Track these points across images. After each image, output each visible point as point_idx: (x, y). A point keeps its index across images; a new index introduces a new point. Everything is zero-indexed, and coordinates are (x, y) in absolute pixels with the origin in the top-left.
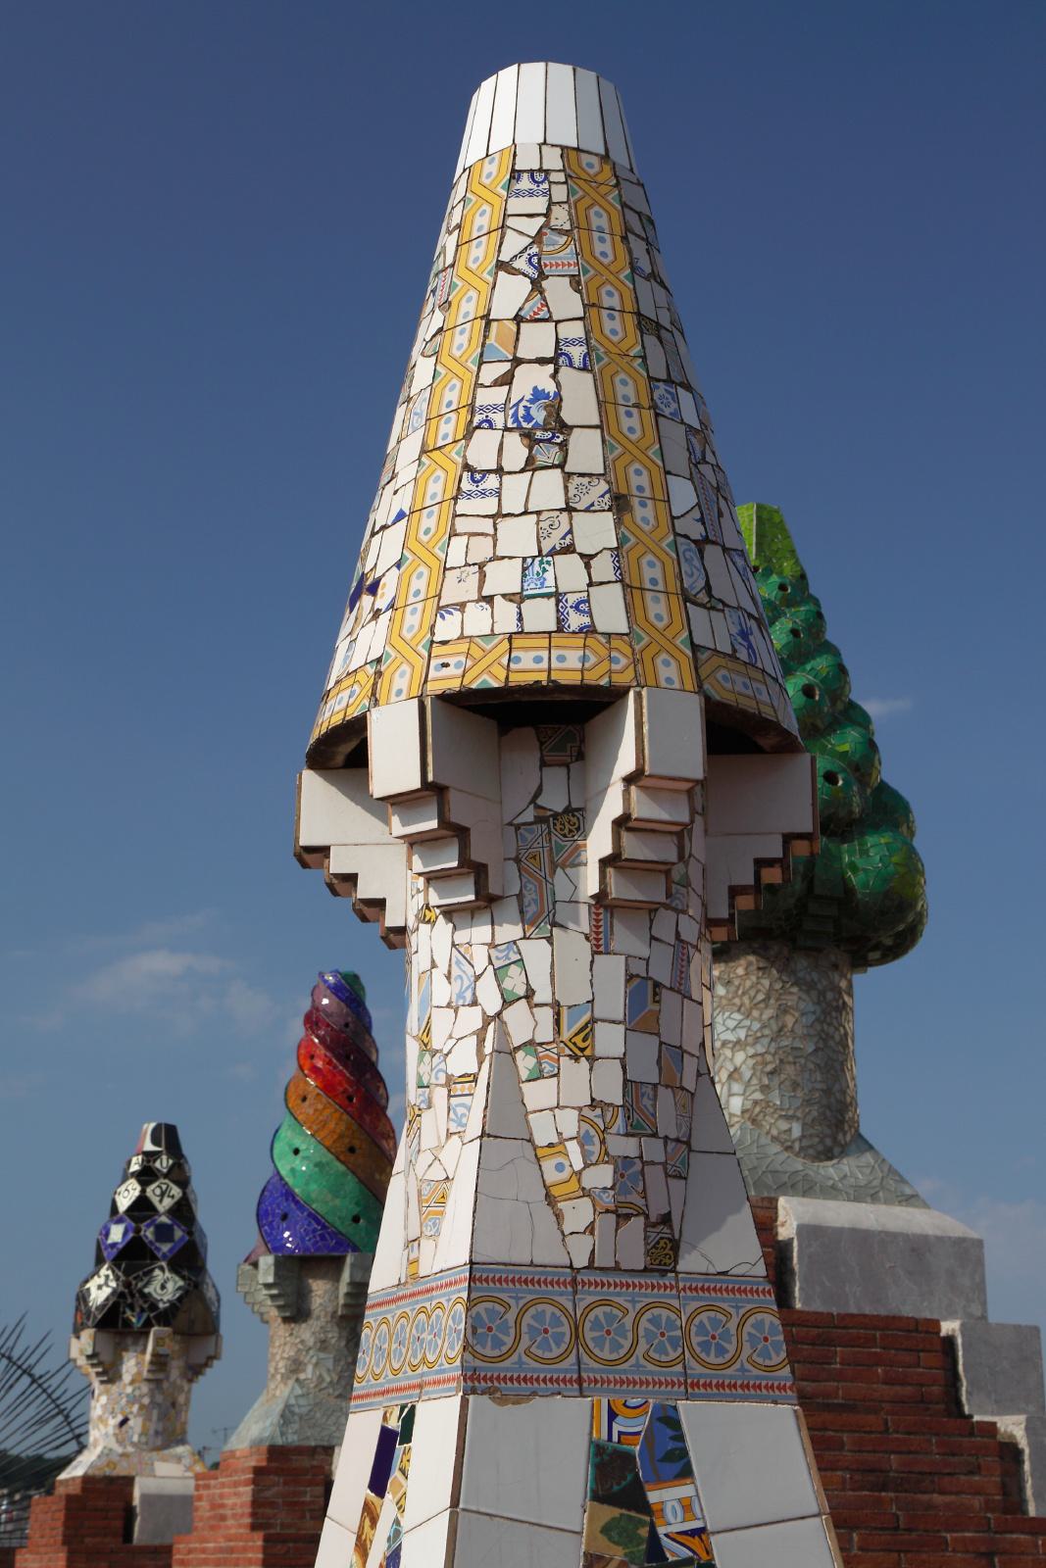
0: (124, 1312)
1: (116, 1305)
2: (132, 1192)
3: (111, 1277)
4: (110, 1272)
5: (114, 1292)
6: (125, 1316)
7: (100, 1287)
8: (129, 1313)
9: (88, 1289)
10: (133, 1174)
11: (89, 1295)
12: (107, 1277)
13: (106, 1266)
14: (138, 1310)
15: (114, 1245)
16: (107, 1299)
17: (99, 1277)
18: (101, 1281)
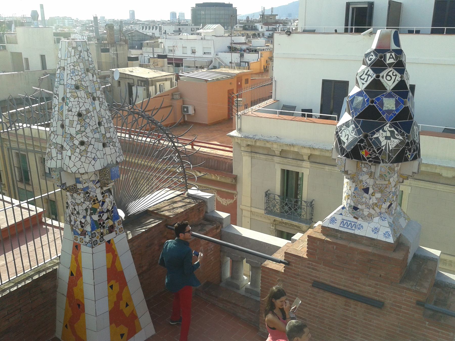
0: (406, 153)
1: (404, 150)
2: (393, 78)
3: (396, 132)
4: (393, 129)
5: (402, 142)
6: (406, 155)
7: (387, 138)
8: (408, 153)
9: (377, 138)
10: (390, 65)
11: (380, 143)
12: (392, 132)
13: (388, 125)
14: (412, 151)
15: (389, 111)
16: (397, 146)
17: (384, 131)
18: (389, 134)
